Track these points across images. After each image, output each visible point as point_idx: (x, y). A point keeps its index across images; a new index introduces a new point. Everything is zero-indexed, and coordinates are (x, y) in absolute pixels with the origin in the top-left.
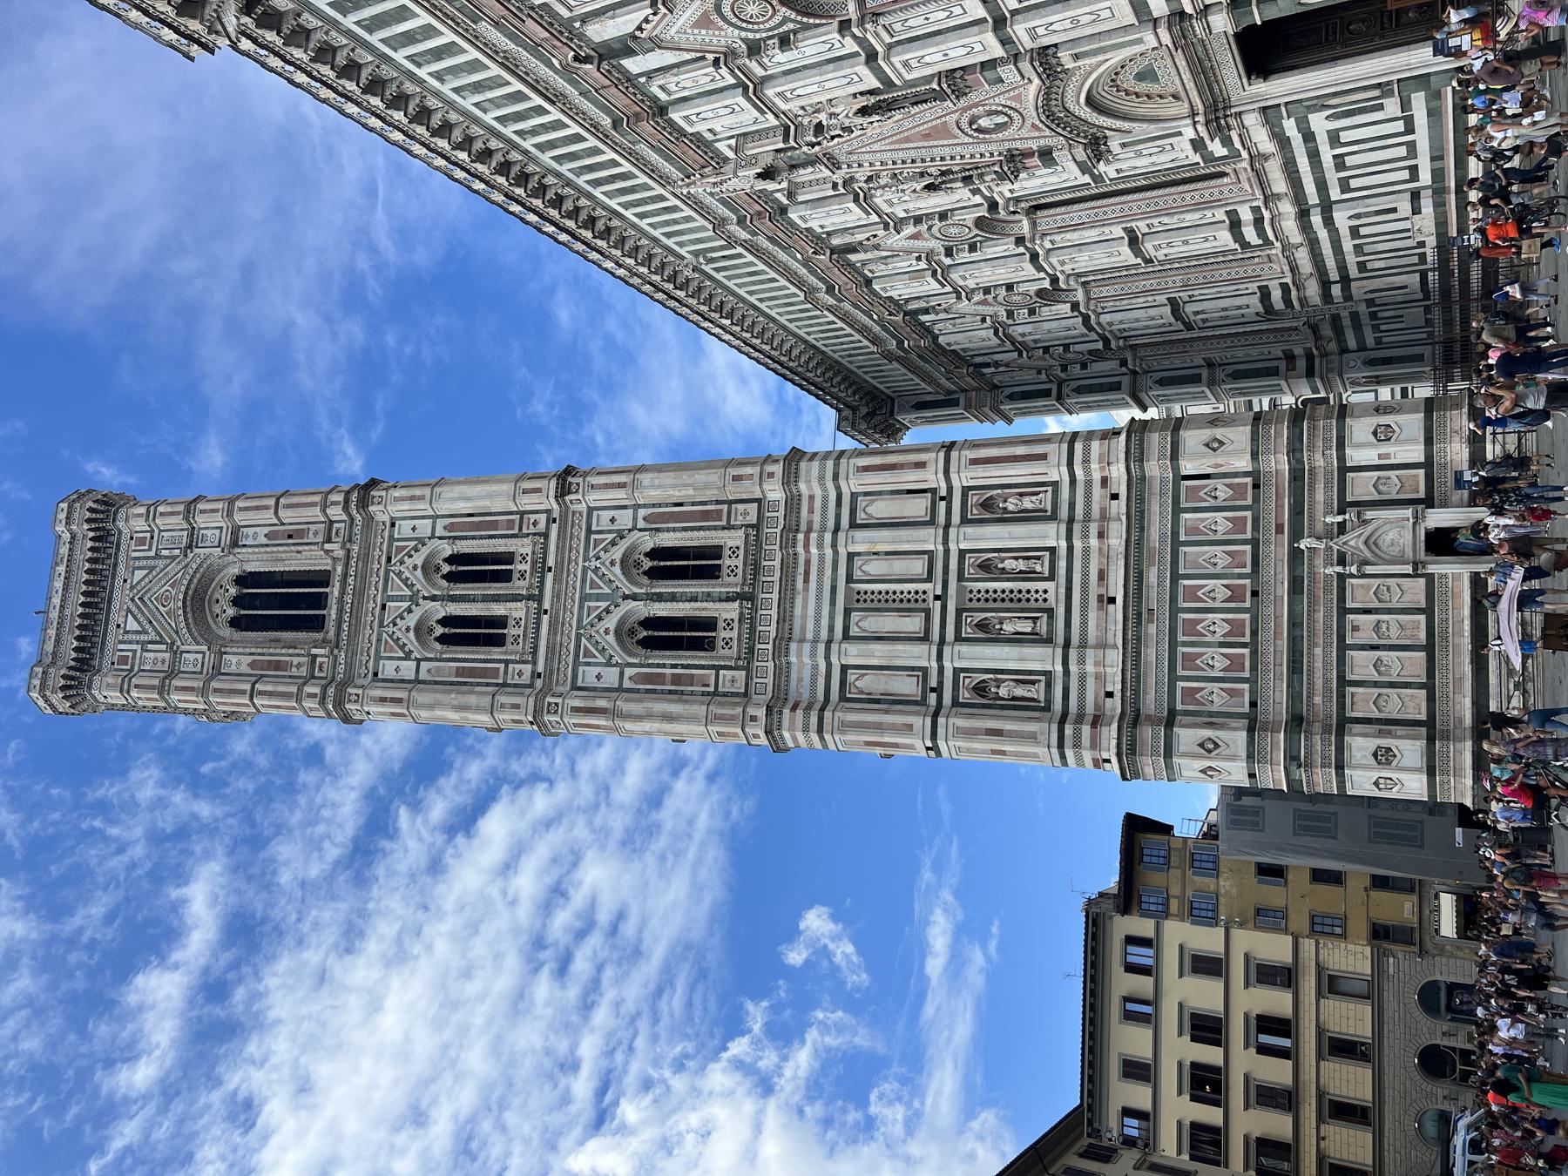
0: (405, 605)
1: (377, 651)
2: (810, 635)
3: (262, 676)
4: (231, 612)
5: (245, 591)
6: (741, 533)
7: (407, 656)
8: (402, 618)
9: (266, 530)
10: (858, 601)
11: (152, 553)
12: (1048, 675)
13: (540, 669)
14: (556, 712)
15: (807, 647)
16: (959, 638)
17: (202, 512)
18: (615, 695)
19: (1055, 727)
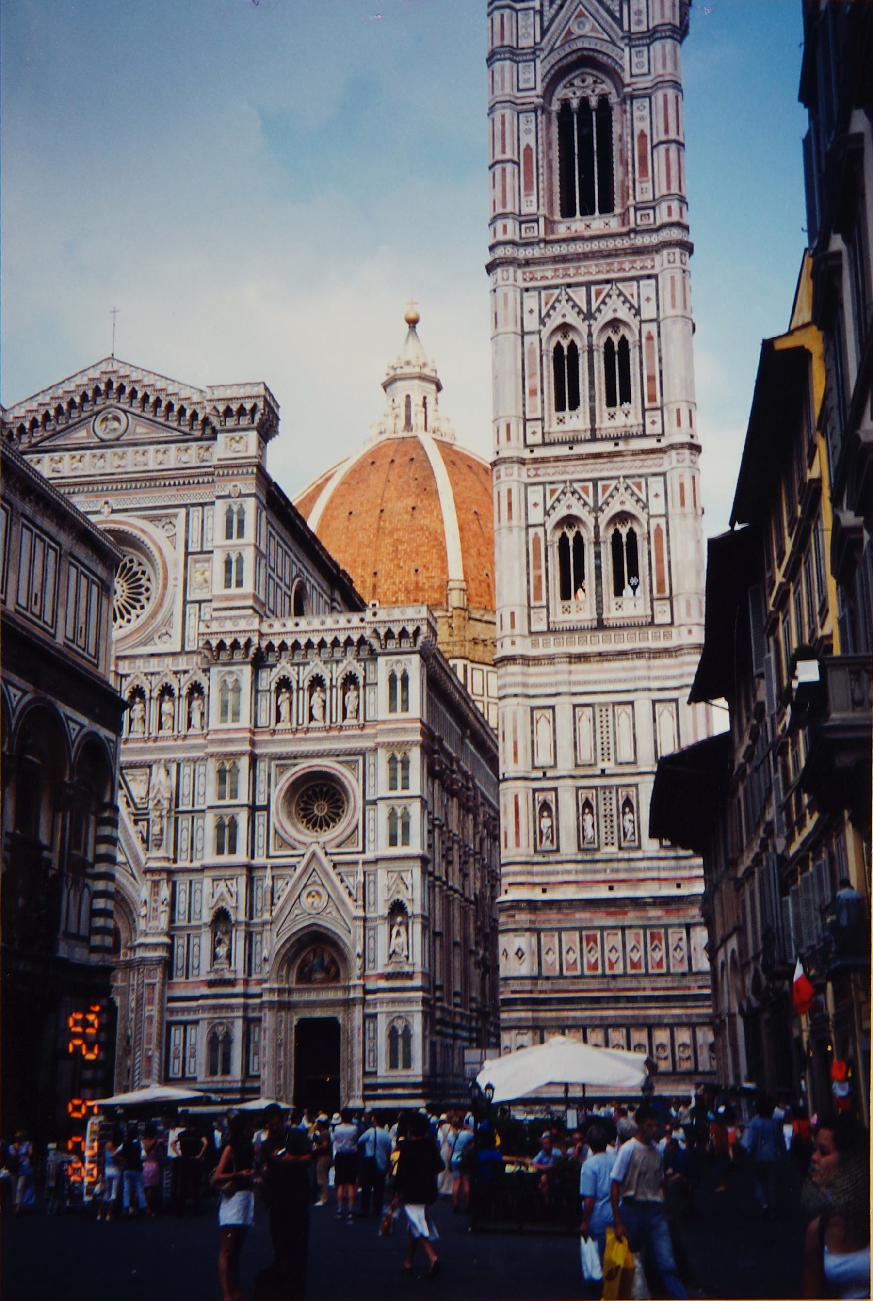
0: (584, 309)
1: (546, 288)
2: (574, 678)
3: (518, 164)
4: (575, 103)
5: (594, 114)
6: (649, 612)
7: (542, 322)
8: (573, 307)
9: (648, 132)
12: (558, 850)
13: (539, 453)
14: (507, 475)
15: (565, 677)
17: (664, 47)
18: (524, 525)
19: (523, 859)
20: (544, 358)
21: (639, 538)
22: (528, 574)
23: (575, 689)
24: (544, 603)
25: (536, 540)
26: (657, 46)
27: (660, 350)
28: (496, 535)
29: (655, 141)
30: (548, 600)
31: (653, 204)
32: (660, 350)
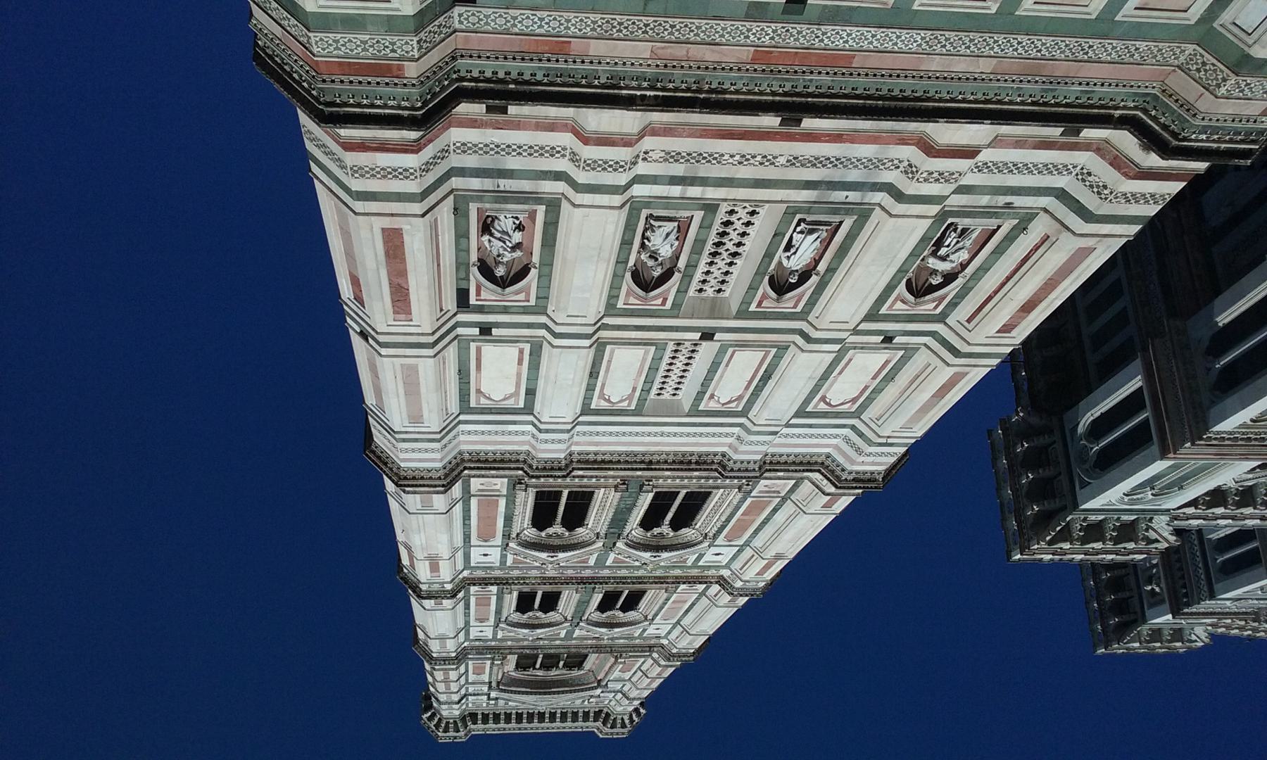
5: (538, 666)
21: (530, 526)
24: (749, 500)
26: (456, 698)
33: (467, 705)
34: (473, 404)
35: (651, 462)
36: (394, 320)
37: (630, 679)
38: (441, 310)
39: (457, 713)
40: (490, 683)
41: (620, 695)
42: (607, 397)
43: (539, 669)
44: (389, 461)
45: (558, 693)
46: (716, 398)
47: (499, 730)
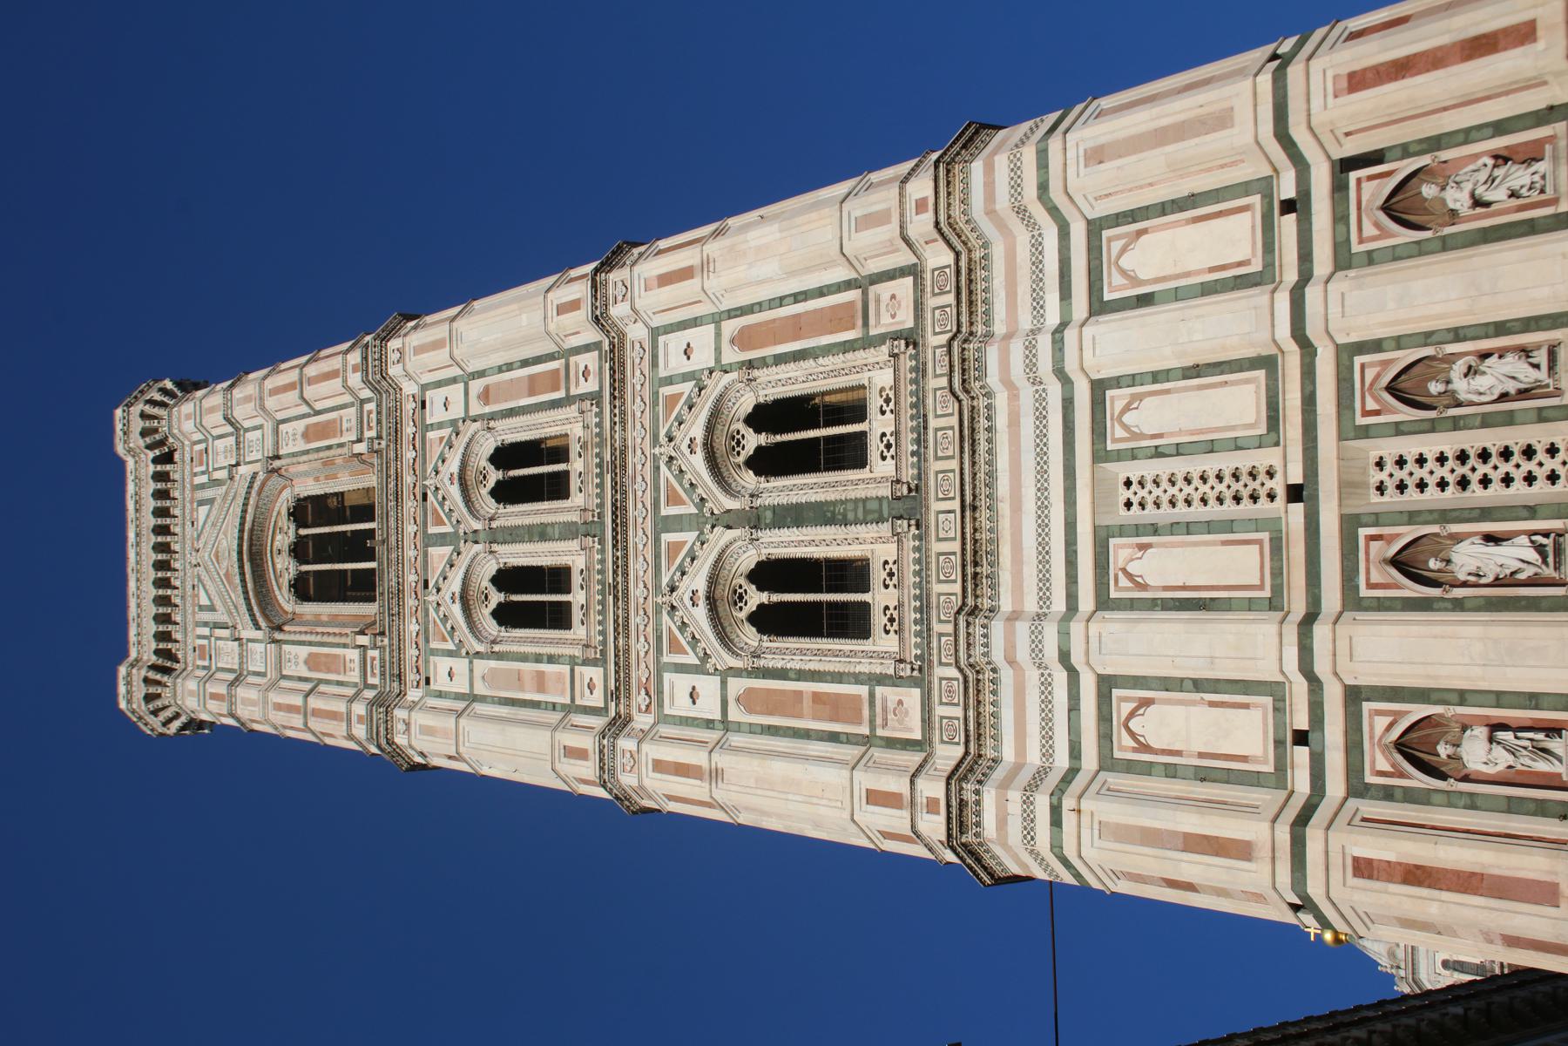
2: (1031, 605)
3: (320, 681)
5: (303, 532)
6: (885, 349)
9: (300, 425)
10: (1128, 504)
11: (204, 479)
16: (1352, 601)
18: (712, 736)
20: (497, 648)
21: (761, 400)
22: (806, 735)
23: (1059, 605)
24: (863, 690)
25: (747, 700)
26: (239, 413)
27: (500, 370)
28: (741, 820)
29: (304, 409)
30: (857, 679)
31: (357, 404)
32: (500, 370)
33: (200, 442)
34: (1106, 234)
35: (974, 508)
36: (1335, 77)
37: (284, 677)
38: (1347, 134)
39: (188, 426)
40: (277, 457)
41: (231, 677)
42: (1135, 405)
43: (297, 534)
44: (972, 149)
45: (242, 574)
46: (1140, 554)
47: (136, 502)
